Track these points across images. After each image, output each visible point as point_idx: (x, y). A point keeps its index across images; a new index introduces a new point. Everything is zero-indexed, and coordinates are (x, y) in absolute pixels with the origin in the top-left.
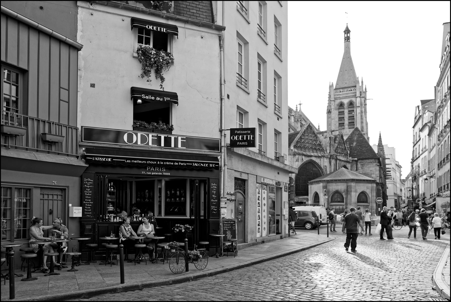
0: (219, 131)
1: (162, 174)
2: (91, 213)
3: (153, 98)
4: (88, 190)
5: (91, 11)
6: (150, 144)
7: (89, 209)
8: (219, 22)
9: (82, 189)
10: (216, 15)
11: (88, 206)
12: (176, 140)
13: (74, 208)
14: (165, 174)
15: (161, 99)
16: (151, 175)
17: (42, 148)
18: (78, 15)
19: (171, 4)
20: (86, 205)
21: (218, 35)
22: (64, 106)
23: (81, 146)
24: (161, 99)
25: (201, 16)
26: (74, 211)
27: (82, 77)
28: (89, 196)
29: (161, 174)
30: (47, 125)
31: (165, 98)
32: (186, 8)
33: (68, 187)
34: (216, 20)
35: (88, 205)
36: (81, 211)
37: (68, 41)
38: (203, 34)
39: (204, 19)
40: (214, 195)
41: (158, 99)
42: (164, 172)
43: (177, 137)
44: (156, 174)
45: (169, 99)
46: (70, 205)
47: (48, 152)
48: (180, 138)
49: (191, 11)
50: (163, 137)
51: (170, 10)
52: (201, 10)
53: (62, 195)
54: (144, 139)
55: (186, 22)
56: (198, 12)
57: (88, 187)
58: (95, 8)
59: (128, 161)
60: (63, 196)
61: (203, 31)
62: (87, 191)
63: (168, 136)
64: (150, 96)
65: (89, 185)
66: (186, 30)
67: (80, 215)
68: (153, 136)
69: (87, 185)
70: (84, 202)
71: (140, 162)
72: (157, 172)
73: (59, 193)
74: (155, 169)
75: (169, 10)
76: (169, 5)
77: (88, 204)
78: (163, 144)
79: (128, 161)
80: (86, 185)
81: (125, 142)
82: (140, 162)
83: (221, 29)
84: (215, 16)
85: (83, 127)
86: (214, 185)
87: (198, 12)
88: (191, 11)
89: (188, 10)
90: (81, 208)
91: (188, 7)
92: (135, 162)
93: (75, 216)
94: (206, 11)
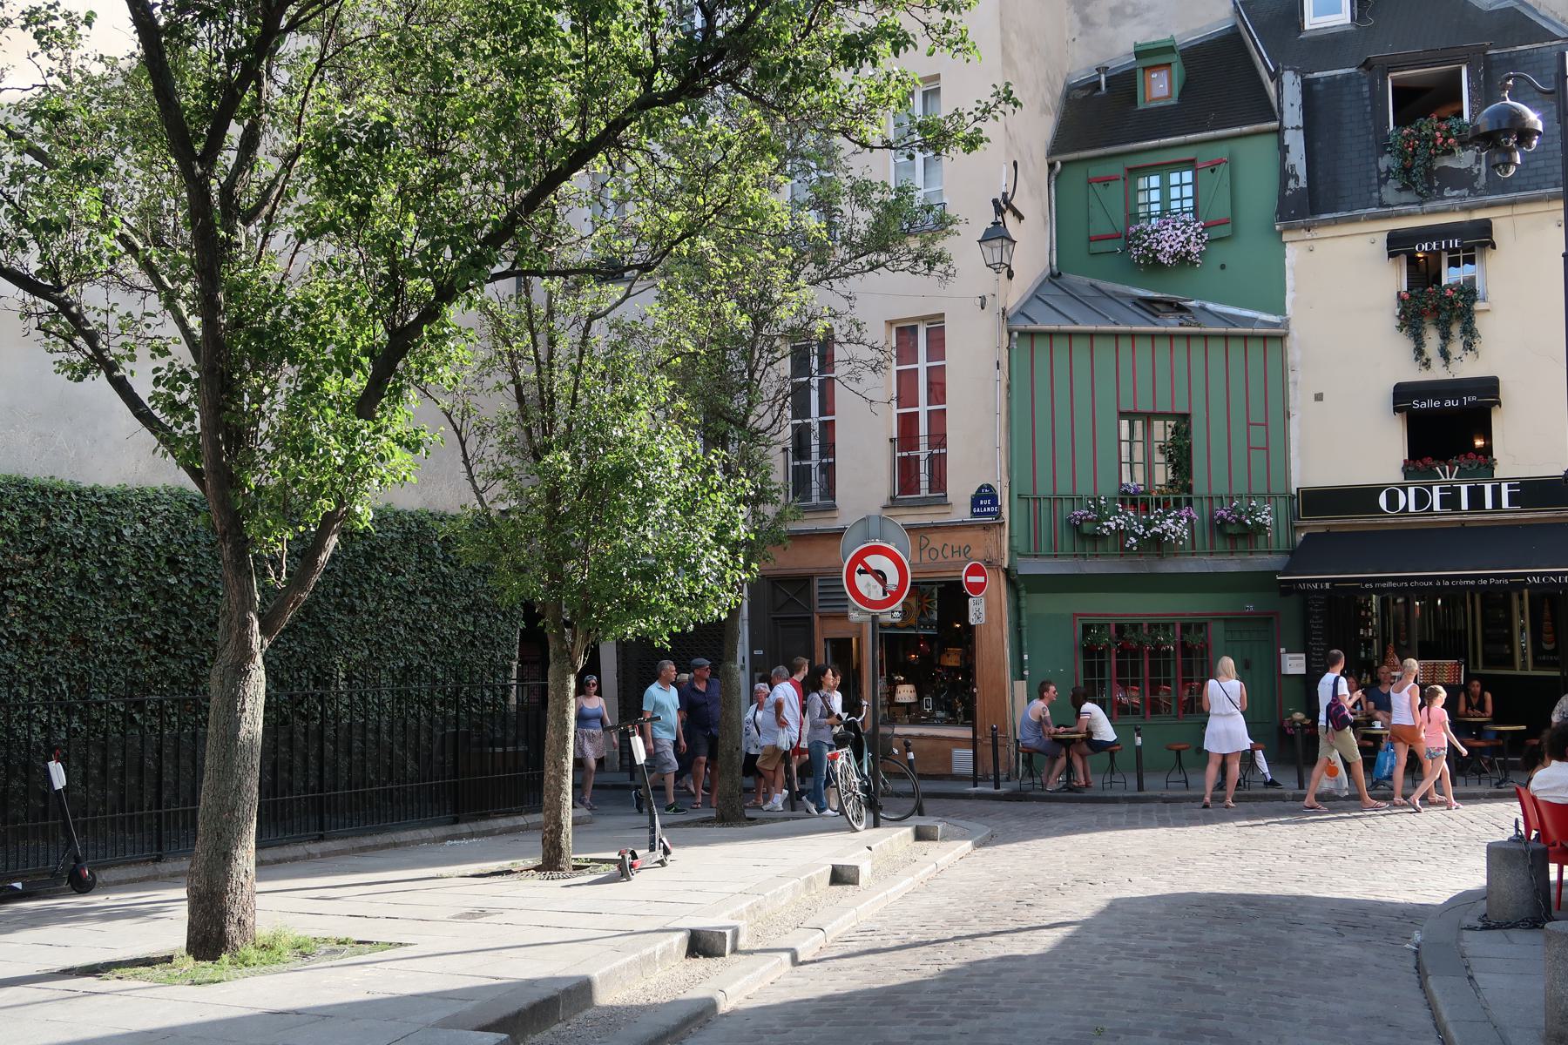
3: (1436, 404)
5: (1309, 243)
6: (1437, 507)
12: (1497, 492)
17: (1219, 545)
22: (1257, 456)
28: (1318, 630)
36: (1304, 662)
41: (1449, 403)
45: (1474, 398)
46: (1282, 650)
48: (1504, 486)
50: (1464, 489)
54: (1422, 499)
67: (1302, 671)
78: (1465, 505)
90: (1303, 655)
93: (1290, 671)
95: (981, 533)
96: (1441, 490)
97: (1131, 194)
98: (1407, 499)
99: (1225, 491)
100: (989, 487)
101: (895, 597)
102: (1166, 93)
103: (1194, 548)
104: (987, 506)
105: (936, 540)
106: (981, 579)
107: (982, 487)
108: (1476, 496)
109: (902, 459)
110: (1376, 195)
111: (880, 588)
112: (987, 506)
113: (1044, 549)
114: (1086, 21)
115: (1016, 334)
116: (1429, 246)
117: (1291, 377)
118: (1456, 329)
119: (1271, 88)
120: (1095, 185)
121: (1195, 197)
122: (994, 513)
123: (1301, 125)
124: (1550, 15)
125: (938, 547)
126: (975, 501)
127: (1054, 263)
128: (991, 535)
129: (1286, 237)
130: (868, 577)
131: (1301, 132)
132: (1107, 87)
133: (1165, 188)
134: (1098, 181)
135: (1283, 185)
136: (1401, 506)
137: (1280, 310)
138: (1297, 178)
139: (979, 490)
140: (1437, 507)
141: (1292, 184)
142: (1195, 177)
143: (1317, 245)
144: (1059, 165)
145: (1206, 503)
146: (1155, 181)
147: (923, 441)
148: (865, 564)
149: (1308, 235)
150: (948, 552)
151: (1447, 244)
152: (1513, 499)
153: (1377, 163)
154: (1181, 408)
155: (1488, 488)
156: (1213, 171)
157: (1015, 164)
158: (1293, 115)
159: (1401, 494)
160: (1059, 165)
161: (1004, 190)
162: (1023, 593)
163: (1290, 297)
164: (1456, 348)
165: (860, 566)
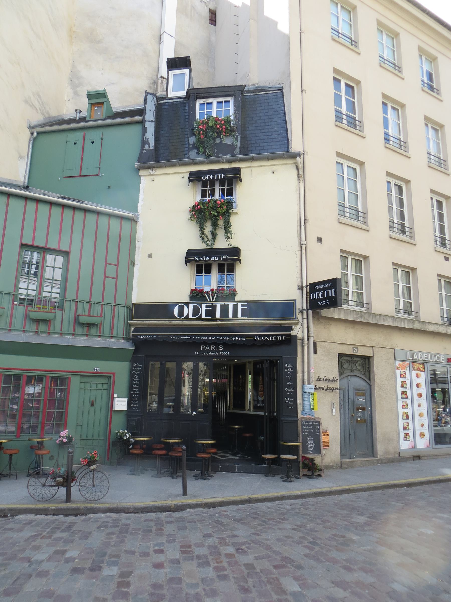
0: (298, 289)
1: (219, 353)
2: (137, 406)
4: (136, 377)
5: (152, 177)
6: (204, 316)
7: (136, 401)
9: (132, 376)
10: (291, 140)
11: (135, 397)
14: (223, 353)
15: (217, 258)
16: (205, 356)
18: (140, 185)
19: (237, 145)
20: (133, 395)
21: (295, 163)
24: (217, 258)
27: (140, 249)
28: (136, 384)
29: (218, 354)
31: (222, 256)
32: (256, 143)
33: (114, 374)
34: (291, 147)
35: (135, 396)
36: (126, 403)
37: (115, 213)
38: (275, 168)
40: (289, 381)
42: (222, 351)
43: (236, 304)
44: (212, 354)
45: (227, 256)
46: (115, 396)
48: (239, 305)
49: (261, 145)
50: (218, 306)
51: (236, 152)
52: (274, 140)
53: (108, 384)
54: (196, 311)
56: (269, 144)
57: (137, 373)
60: (109, 385)
61: (274, 165)
62: (135, 378)
63: (224, 303)
64: (204, 257)
65: (138, 372)
66: (253, 169)
67: (125, 408)
69: (136, 371)
70: (131, 392)
72: (213, 351)
73: (105, 381)
74: (210, 348)
75: (234, 152)
76: (234, 146)
77: (135, 394)
80: (134, 372)
83: (294, 156)
84: (290, 142)
85: (134, 304)
88: (261, 145)
90: (126, 399)
91: (257, 142)
94: (280, 140)
96: (207, 306)
98: (189, 311)
108: (225, 310)
116: (209, 177)
117: (137, 244)
118: (221, 223)
127: (26, 181)
129: (142, 172)
135: (143, 148)
136: (185, 315)
138: (149, 145)
140: (204, 316)
141: (146, 147)
143: (157, 178)
145: (74, 304)
149: (152, 173)
151: (218, 176)
155: (231, 306)
159: (186, 307)
163: (140, 204)
164: (221, 233)
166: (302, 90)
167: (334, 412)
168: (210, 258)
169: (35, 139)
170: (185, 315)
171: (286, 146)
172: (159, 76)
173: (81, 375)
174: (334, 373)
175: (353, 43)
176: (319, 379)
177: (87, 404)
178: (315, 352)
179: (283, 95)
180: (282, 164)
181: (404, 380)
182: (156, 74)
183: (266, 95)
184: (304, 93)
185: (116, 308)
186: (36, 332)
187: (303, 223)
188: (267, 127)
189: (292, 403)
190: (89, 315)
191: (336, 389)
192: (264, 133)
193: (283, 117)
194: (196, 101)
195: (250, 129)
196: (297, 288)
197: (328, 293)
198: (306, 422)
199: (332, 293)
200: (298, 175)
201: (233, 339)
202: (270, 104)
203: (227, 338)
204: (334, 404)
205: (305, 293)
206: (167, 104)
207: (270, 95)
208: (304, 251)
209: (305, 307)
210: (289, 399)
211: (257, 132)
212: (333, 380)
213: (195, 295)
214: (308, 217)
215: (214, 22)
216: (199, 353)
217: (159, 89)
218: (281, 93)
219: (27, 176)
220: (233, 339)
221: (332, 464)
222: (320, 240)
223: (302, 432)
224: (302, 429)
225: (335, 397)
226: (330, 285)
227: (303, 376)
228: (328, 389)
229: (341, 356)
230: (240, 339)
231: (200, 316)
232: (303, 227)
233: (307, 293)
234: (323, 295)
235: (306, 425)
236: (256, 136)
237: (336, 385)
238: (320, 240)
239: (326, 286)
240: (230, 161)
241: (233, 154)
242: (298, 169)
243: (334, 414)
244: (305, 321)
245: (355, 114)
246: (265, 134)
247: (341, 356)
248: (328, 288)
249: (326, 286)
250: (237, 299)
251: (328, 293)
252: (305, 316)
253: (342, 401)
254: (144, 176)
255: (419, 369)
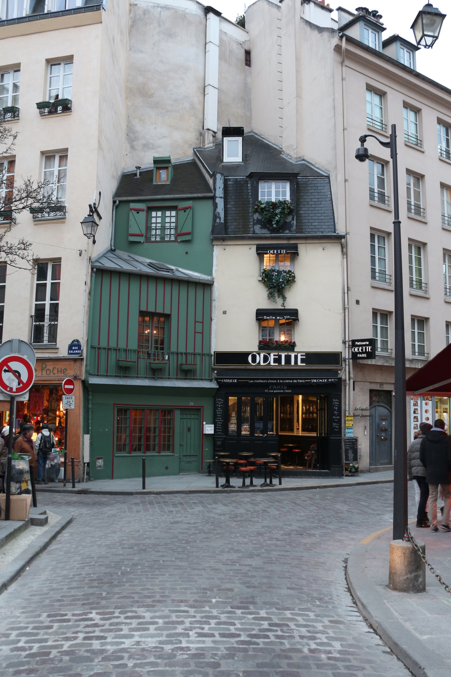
5: (224, 246)
6: (272, 364)
8: (341, 230)
11: (219, 424)
12: (296, 357)
13: (207, 425)
14: (286, 391)
16: (273, 393)
19: (293, 223)
21: (340, 243)
22: (199, 336)
23: (213, 370)
25: (323, 227)
26: (207, 428)
28: (220, 414)
30: (184, 356)
33: (203, 407)
36: (213, 428)
38: (324, 245)
39: (327, 230)
42: (286, 389)
45: (289, 317)
46: (204, 423)
47: (186, 379)
48: (299, 355)
49: (313, 224)
50: (283, 355)
52: (323, 221)
54: (266, 359)
55: (306, 238)
56: (320, 224)
58: (226, 244)
59: (251, 381)
67: (212, 432)
68: (274, 355)
69: (219, 405)
71: (262, 381)
72: (279, 389)
74: (277, 387)
75: (292, 229)
77: (219, 422)
79: (251, 381)
81: (249, 363)
82: (262, 381)
83: (339, 238)
84: (336, 225)
86: (336, 400)
87: (320, 224)
88: (313, 224)
89: (310, 224)
90: (213, 425)
91: (310, 221)
92: (258, 381)
93: (207, 432)
95: (72, 363)
97: (148, 218)
98: (260, 359)
99: (184, 351)
100: (78, 341)
101: (25, 386)
102: (165, 179)
103: (169, 375)
104: (76, 350)
105: (50, 366)
106: (71, 387)
107: (74, 341)
108: (288, 358)
109: (36, 326)
110: (252, 229)
111: (17, 381)
112: (76, 350)
113: (102, 371)
114: (132, 147)
115: (95, 270)
117: (214, 303)
119: (211, 181)
120: (133, 211)
121: (177, 222)
122: (79, 353)
123: (223, 196)
124: (320, 167)
125: (51, 368)
126: (70, 347)
127: (113, 245)
128: (78, 364)
130: (10, 374)
131: (223, 200)
132: (140, 175)
133: (164, 217)
134: (135, 210)
136: (257, 362)
137: (211, 274)
139: (73, 342)
140: (272, 364)
141: (218, 220)
142: (177, 214)
143: (227, 248)
144: (118, 201)
145: (175, 356)
146: (159, 214)
147: (47, 317)
148: (8, 367)
149: (224, 243)
150: (55, 371)
151: (281, 251)
152: (303, 361)
153: (253, 216)
154: (167, 311)
156: (185, 211)
157: (100, 193)
158: (219, 192)
159: (258, 356)
160: (118, 201)
161: (94, 202)
162: (90, 393)
165: (5, 368)
166: (346, 181)
167: (366, 432)
168: (276, 317)
169: (117, 207)
170: (257, 362)
171: (333, 227)
172: (205, 128)
173: (181, 409)
174: (366, 404)
175: (384, 126)
176: (356, 409)
177: (185, 430)
178: (354, 389)
179: (329, 180)
180: (330, 243)
181: (416, 407)
182: (201, 125)
183: (315, 180)
184: (346, 183)
185: (204, 357)
186: (153, 378)
187: (346, 291)
188: (317, 209)
189: (338, 427)
190: (186, 364)
191: (368, 416)
192: (315, 213)
193: (330, 201)
194: (258, 183)
195: (304, 209)
196: (342, 342)
197: (366, 348)
198: (347, 439)
199: (369, 349)
200: (342, 251)
201: (296, 381)
202: (319, 188)
203: (291, 381)
204: (365, 427)
205: (347, 346)
206: (232, 180)
207: (318, 180)
208: (347, 313)
209: (347, 357)
210: (336, 424)
211: (310, 212)
212: (365, 410)
213: (262, 346)
214: (350, 286)
215: (248, 62)
216: (269, 391)
217: (206, 142)
218: (328, 179)
219: (113, 240)
220: (296, 381)
221: (363, 469)
222: (358, 302)
223: (345, 447)
224: (345, 444)
225: (367, 422)
226: (368, 343)
227: (345, 407)
228: (362, 416)
229: (371, 391)
230: (301, 381)
231: (269, 363)
232: (346, 295)
233: (349, 345)
234: (362, 350)
235: (347, 442)
236: (308, 216)
237: (367, 413)
238: (358, 302)
239: (364, 343)
240: (289, 238)
241: (290, 231)
242: (342, 248)
243: (366, 434)
244: (347, 367)
245: (384, 190)
246: (316, 215)
247: (371, 391)
248: (366, 345)
249: (364, 343)
250: (296, 349)
251: (366, 348)
252: (347, 363)
253: (371, 424)
254: (217, 245)
255: (428, 399)
